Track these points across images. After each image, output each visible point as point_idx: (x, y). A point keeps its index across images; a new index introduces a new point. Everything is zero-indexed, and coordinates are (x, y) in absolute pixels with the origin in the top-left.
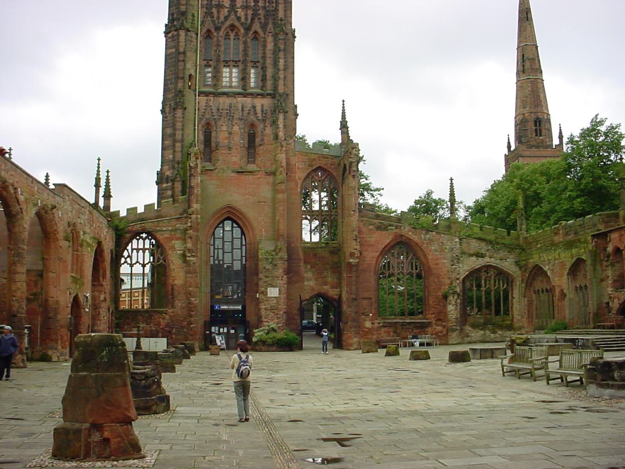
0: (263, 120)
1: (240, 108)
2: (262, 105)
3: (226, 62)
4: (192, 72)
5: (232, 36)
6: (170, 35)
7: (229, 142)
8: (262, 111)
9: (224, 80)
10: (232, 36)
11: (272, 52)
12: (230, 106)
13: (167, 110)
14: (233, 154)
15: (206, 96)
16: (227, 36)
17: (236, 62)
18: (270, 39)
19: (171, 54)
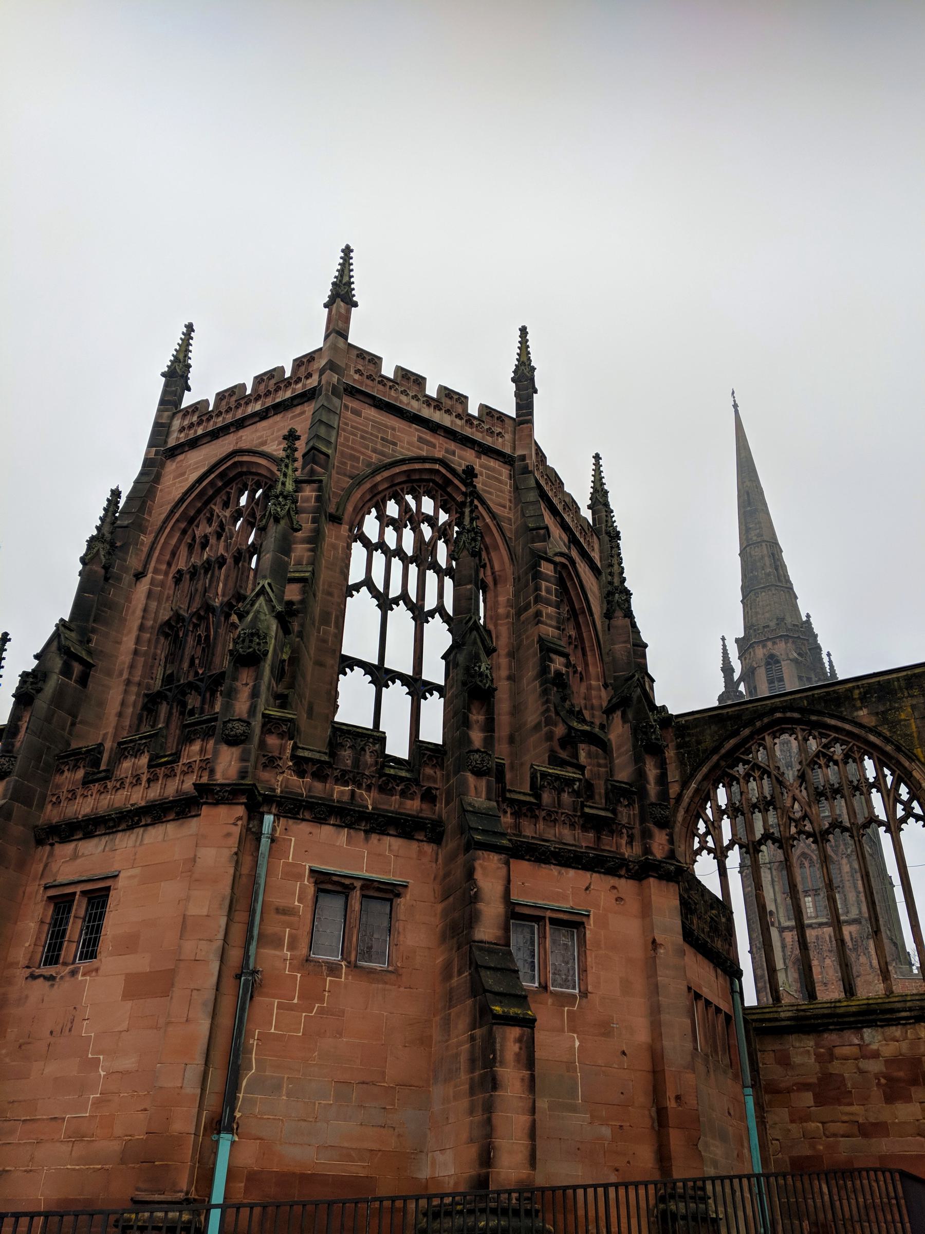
0: (854, 949)
1: (828, 939)
2: (850, 933)
3: (806, 892)
4: (774, 910)
5: (807, 864)
6: (744, 874)
7: (823, 978)
8: (852, 939)
9: (809, 911)
10: (807, 864)
11: (850, 874)
12: (817, 937)
13: (754, 950)
14: (830, 990)
15: (791, 931)
16: (802, 866)
17: (816, 890)
18: (844, 861)
19: (749, 892)
